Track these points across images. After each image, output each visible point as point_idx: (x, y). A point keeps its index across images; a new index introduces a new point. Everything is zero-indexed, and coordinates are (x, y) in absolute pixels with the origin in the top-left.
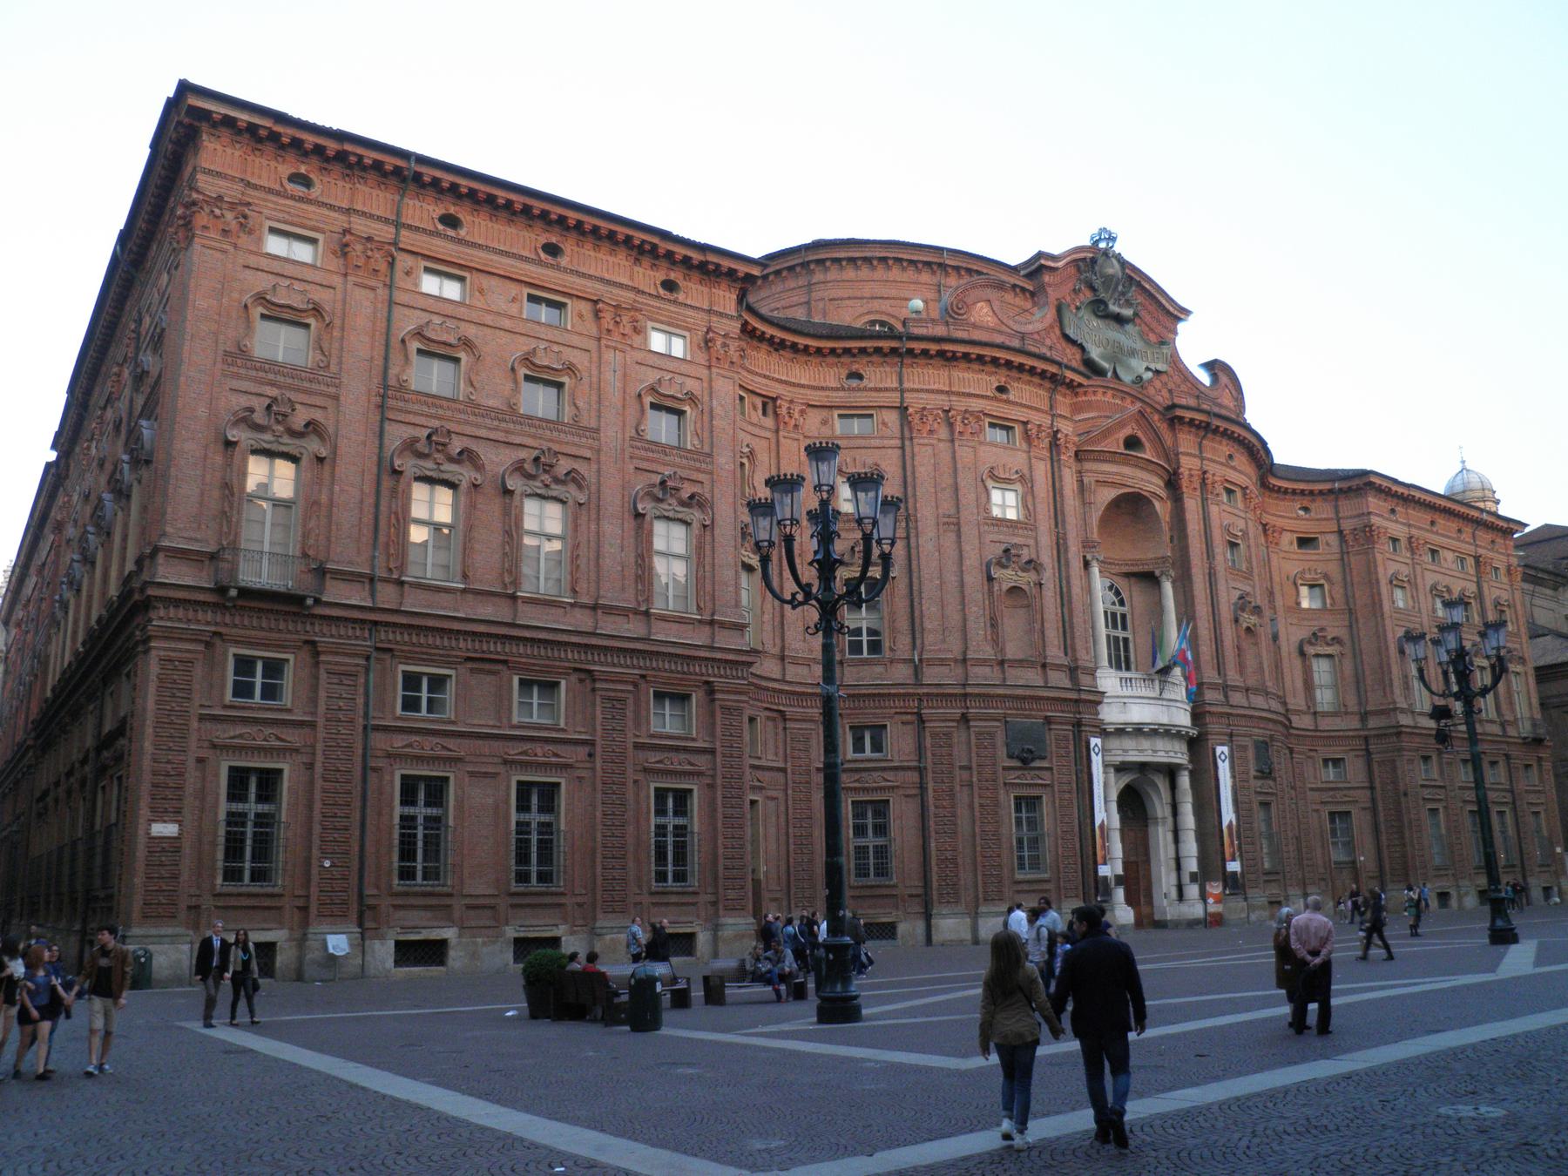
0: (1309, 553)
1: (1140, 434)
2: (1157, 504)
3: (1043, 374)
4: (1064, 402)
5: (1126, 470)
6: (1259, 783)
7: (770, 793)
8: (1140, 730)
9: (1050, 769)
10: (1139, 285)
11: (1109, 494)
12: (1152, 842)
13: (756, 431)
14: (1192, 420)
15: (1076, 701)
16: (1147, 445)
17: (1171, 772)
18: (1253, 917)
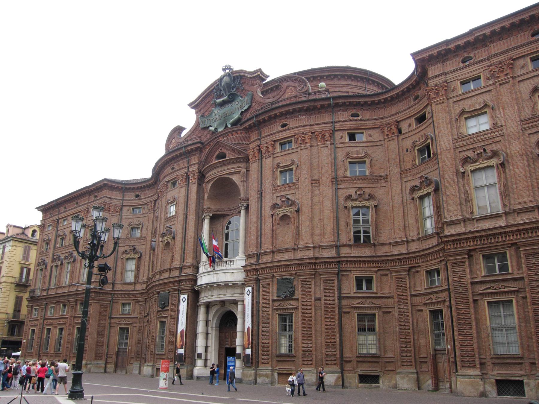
0: (424, 125)
1: (224, 150)
2: (235, 178)
3: (181, 155)
4: (195, 160)
5: (214, 171)
6: (276, 304)
7: (135, 325)
8: (212, 286)
9: (168, 310)
10: (241, 77)
11: (210, 185)
12: (218, 338)
13: (144, 215)
14: (250, 125)
15: (179, 281)
16: (227, 153)
17: (235, 303)
18: (259, 380)
